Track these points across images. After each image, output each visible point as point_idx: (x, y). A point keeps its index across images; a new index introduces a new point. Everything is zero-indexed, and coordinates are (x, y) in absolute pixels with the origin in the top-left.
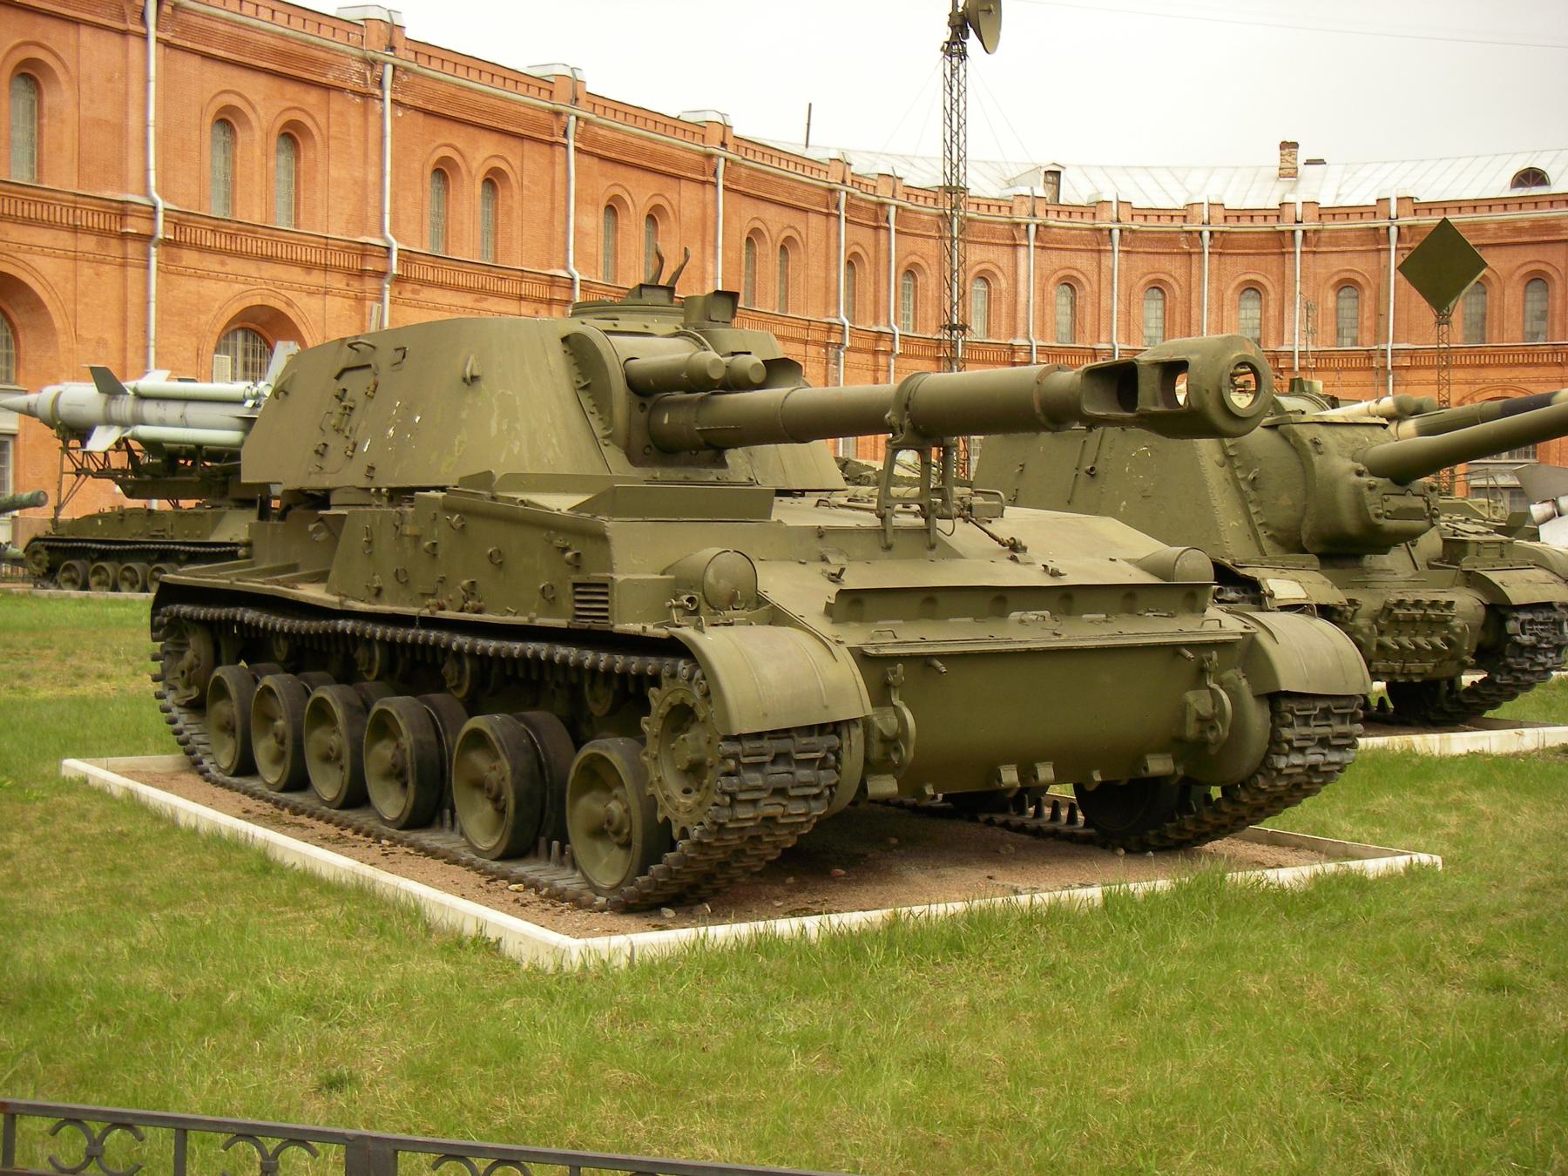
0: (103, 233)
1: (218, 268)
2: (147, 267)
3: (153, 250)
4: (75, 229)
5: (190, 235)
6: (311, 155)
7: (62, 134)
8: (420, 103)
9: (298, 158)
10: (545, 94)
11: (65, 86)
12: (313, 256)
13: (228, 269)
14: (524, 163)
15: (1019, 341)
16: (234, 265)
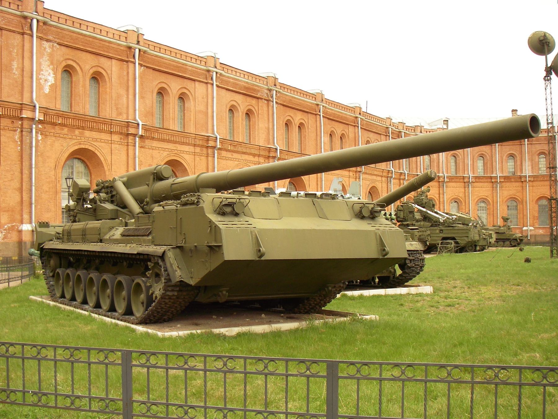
0: (202, 146)
1: (230, 156)
2: (214, 157)
3: (216, 151)
4: (195, 145)
5: (225, 146)
6: (254, 119)
7: (191, 116)
8: (282, 103)
9: (250, 121)
10: (314, 99)
11: (191, 101)
12: (256, 152)
13: (233, 157)
14: (309, 121)
15: (441, 175)
16: (236, 156)
